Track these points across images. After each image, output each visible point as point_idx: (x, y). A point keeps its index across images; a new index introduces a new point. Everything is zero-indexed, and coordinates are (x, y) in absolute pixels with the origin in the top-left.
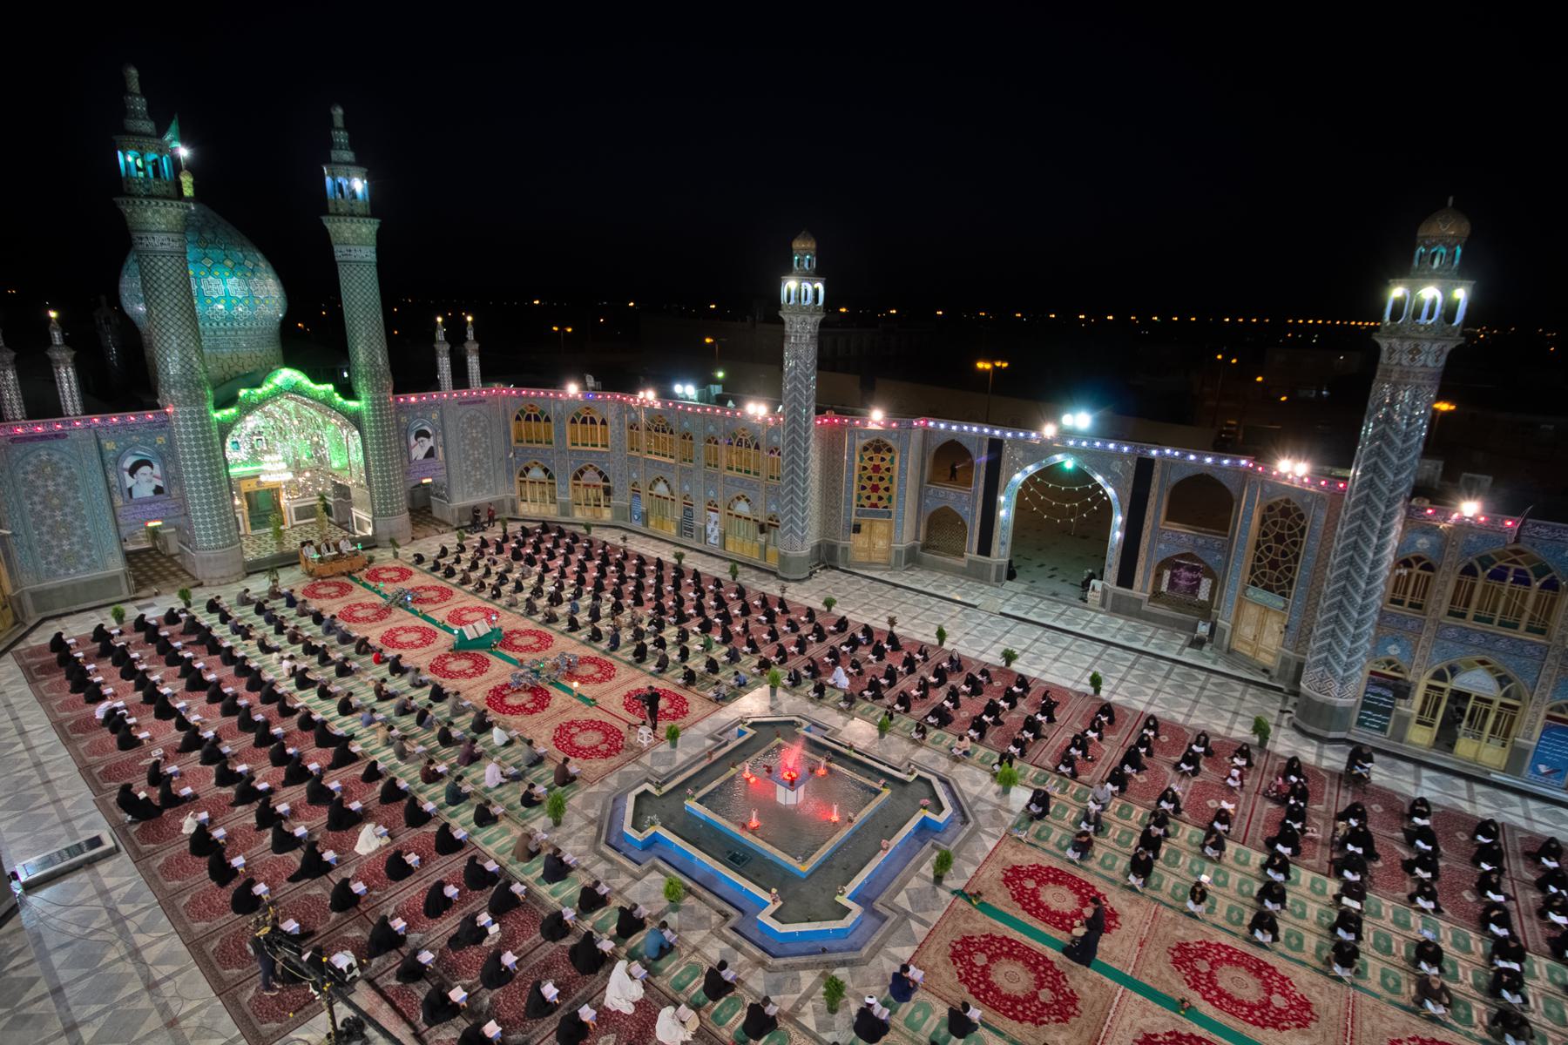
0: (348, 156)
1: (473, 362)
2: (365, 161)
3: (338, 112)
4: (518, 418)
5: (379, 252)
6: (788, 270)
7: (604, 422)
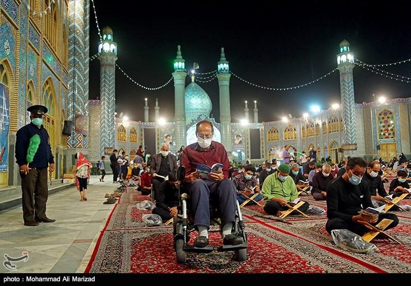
0: (224, 59)
1: (256, 115)
2: (229, 59)
3: (223, 49)
4: (269, 132)
5: (230, 83)
6: (339, 53)
7: (295, 130)
